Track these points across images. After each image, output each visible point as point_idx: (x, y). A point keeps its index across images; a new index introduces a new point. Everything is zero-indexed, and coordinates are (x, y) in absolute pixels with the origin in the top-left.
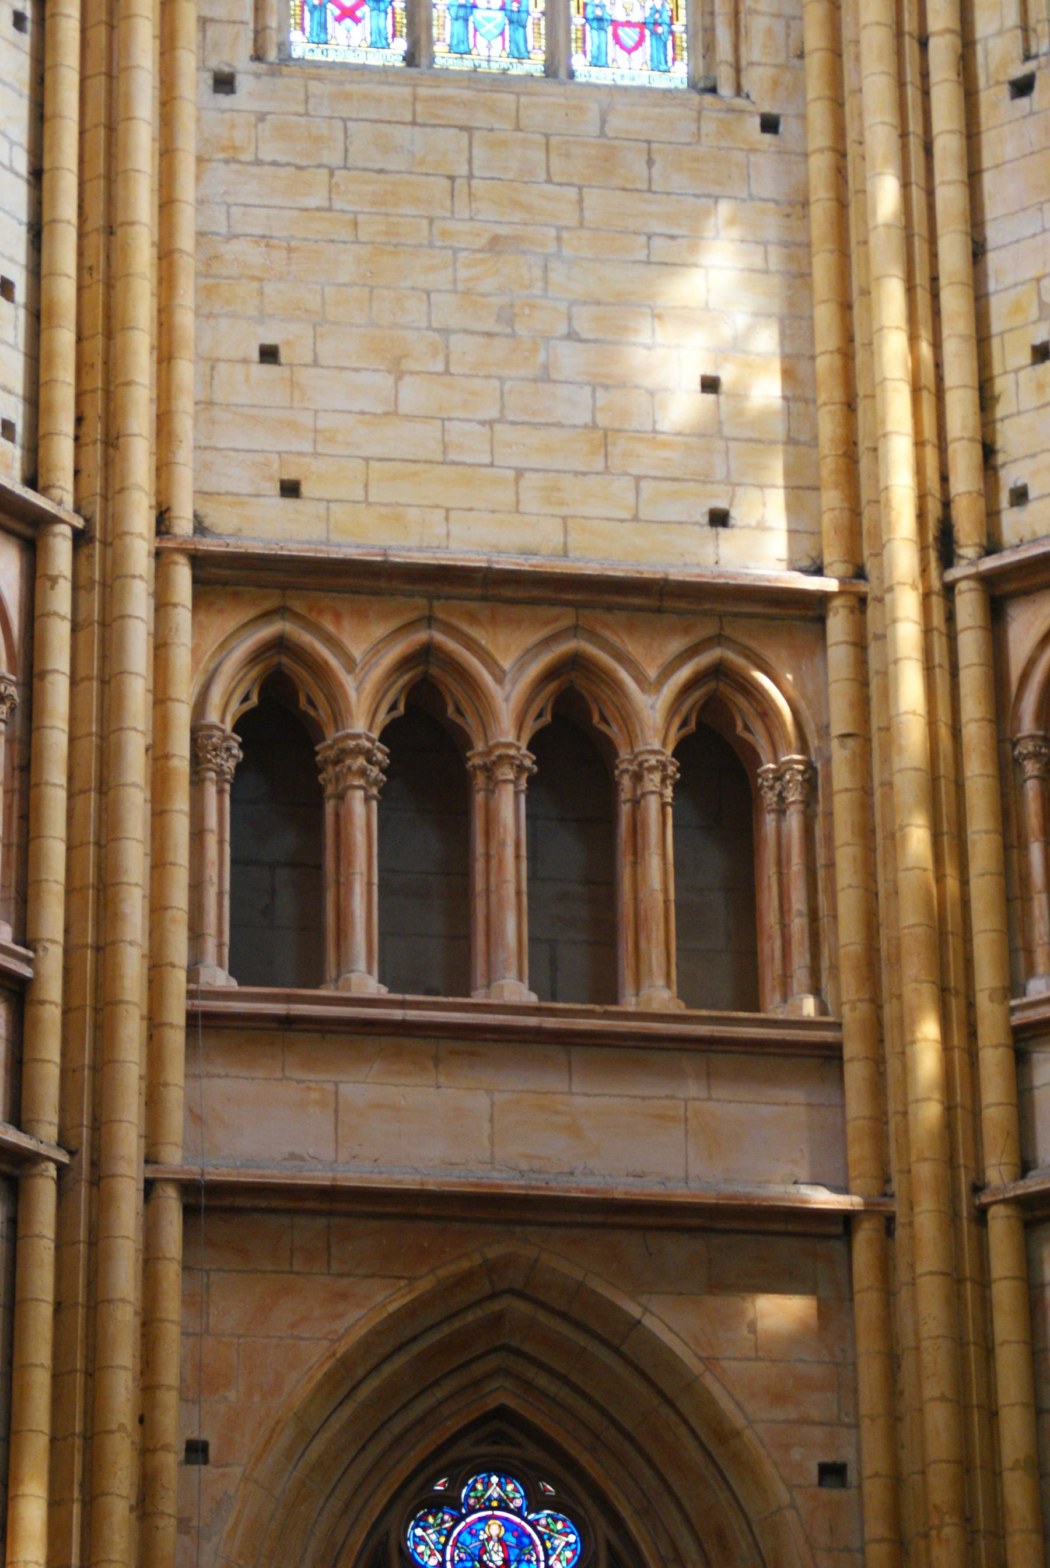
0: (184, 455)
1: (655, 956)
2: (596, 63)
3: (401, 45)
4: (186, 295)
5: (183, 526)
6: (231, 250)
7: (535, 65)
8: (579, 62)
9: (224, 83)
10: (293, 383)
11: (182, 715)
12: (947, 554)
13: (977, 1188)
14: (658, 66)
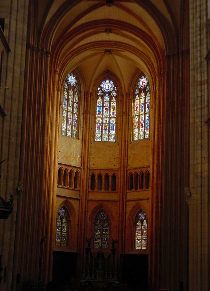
2: (111, 140)
3: (101, 140)
7: (107, 140)
8: (110, 140)
9: (91, 143)
10: (94, 159)
11: (88, 177)
13: (124, 200)
14: (114, 140)
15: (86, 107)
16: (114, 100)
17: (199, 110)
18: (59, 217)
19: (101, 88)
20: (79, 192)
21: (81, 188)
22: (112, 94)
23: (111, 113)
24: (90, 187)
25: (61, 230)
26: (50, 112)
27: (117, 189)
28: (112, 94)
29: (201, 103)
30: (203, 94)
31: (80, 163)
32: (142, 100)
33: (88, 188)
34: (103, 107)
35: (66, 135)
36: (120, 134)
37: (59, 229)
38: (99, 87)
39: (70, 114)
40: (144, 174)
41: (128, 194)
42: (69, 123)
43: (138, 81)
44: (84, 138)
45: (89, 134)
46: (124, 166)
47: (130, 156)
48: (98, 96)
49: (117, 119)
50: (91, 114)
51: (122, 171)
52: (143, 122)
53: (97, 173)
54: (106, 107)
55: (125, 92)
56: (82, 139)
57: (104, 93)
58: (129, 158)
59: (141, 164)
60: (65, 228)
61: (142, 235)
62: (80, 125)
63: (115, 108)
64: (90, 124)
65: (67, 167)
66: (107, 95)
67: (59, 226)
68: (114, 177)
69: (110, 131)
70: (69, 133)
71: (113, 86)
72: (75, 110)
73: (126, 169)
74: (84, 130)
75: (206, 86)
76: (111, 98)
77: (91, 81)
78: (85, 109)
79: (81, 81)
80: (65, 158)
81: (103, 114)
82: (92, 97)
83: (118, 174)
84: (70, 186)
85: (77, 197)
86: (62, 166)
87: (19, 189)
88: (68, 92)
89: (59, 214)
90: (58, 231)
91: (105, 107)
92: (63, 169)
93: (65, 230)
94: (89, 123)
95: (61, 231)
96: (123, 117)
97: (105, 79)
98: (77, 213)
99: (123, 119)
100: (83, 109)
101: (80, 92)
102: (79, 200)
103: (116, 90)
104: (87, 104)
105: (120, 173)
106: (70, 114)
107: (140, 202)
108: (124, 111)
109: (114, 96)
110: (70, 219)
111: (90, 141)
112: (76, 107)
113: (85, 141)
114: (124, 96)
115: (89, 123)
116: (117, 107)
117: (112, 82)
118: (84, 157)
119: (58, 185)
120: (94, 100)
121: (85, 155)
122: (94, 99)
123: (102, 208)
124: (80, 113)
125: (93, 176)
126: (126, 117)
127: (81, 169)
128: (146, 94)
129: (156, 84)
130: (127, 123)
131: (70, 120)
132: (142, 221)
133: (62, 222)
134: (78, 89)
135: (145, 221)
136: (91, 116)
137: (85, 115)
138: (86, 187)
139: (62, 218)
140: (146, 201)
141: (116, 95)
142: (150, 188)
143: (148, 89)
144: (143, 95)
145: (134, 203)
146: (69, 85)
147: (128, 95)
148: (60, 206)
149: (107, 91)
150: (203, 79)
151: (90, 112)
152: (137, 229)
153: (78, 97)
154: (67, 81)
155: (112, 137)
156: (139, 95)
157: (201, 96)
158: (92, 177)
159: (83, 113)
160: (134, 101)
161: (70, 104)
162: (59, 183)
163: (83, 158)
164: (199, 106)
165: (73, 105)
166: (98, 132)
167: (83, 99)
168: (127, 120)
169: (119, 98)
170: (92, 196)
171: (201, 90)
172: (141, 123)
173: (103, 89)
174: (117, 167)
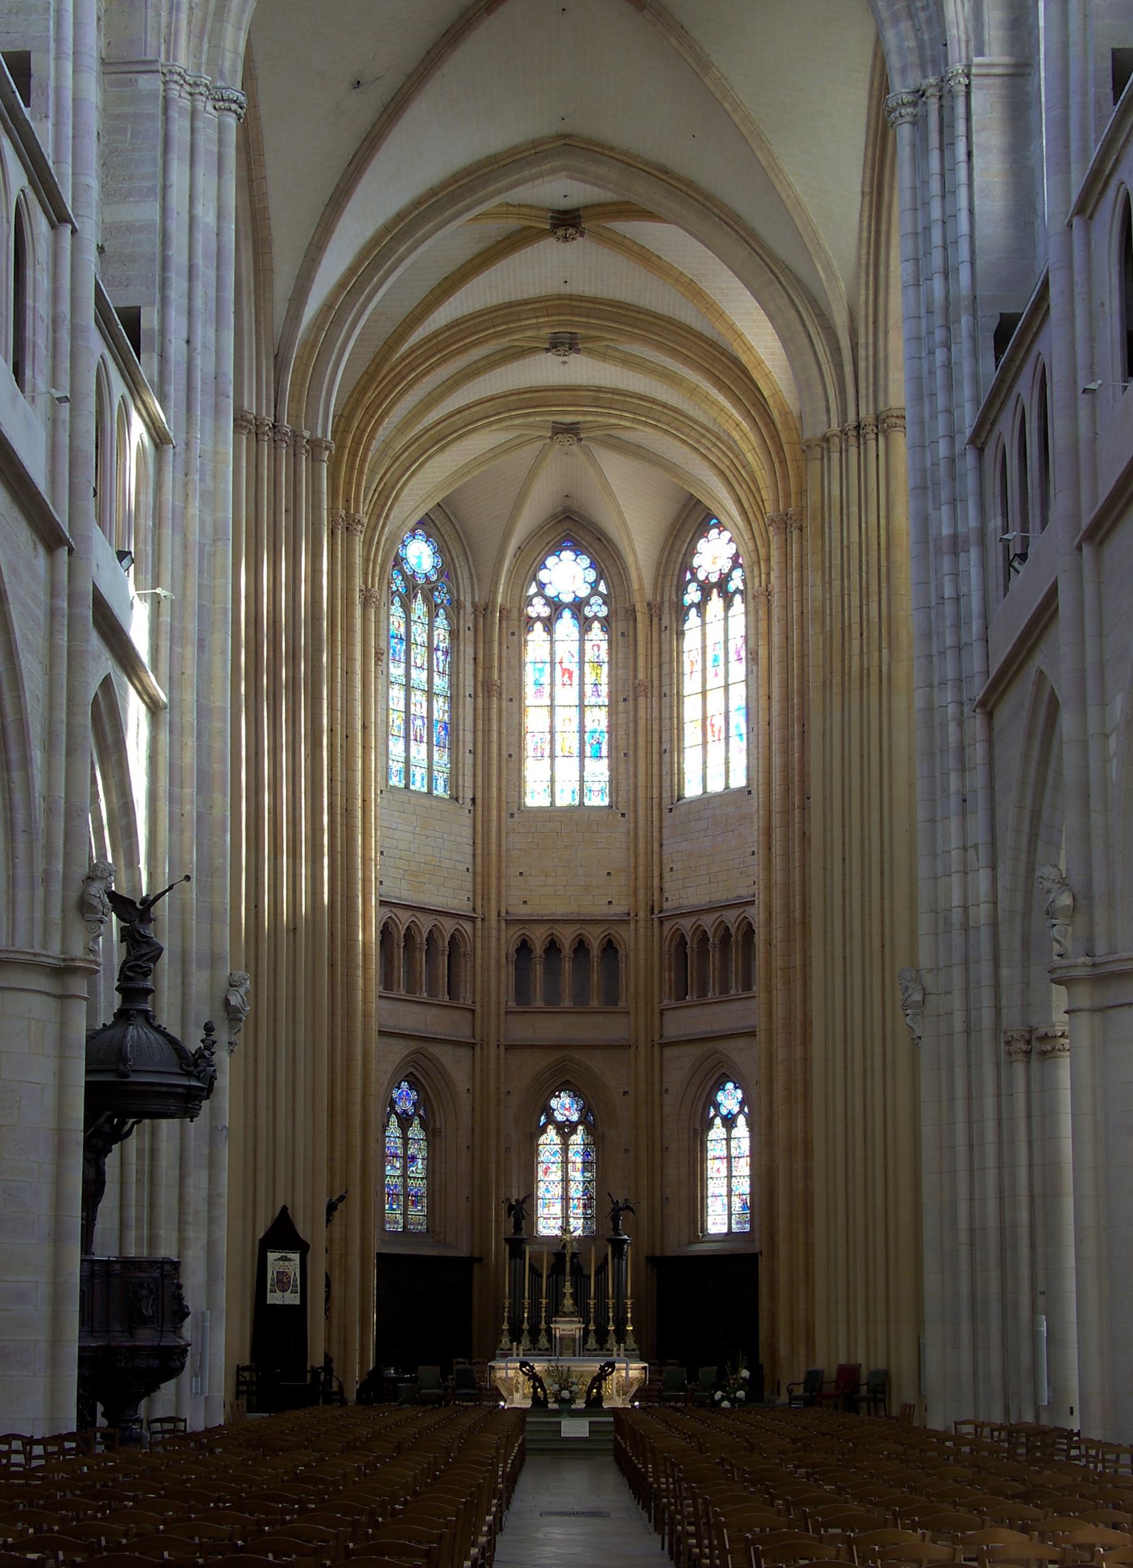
0: (503, 899)
1: (595, 995)
4: (504, 865)
5: (503, 913)
6: (514, 852)
9: (512, 815)
11: (503, 953)
12: (652, 913)
15: (483, 663)
16: (596, 632)
17: (950, 655)
18: (393, 1118)
19: (542, 586)
20: (468, 1015)
21: (478, 998)
22: (588, 612)
23: (588, 689)
24: (512, 988)
25: (405, 1168)
26: (337, 692)
27: (624, 998)
28: (588, 612)
29: (957, 626)
30: (963, 589)
32: (715, 632)
33: (503, 999)
34: (552, 664)
35: (407, 786)
36: (628, 770)
37: (393, 1167)
38: (534, 584)
39: (418, 698)
40: (733, 931)
41: (668, 1016)
42: (416, 735)
43: (692, 551)
44: (479, 796)
45: (499, 778)
46: (650, 902)
47: (673, 861)
48: (530, 622)
49: (612, 709)
50: (504, 696)
51: (641, 924)
52: (719, 722)
53: (538, 937)
54: (564, 666)
55: (642, 596)
56: (474, 800)
57: (556, 606)
58: (669, 870)
59: (720, 894)
60: (420, 1161)
61: (730, 1177)
63: (605, 667)
64: (504, 736)
66: (567, 614)
67: (396, 1156)
68: (610, 947)
69: (587, 761)
70: (418, 778)
71: (592, 575)
72: (441, 683)
73: (657, 915)
74: (479, 762)
75: (974, 554)
76: (585, 625)
77: (499, 562)
78: (480, 678)
79: (459, 562)
80: (406, 877)
81: (552, 696)
82: (504, 623)
83: (625, 936)
84: (432, 991)
85: (464, 1034)
86: (394, 910)
87: (235, 1000)
88: (407, 609)
89: (392, 1103)
90: (392, 1173)
91: (561, 663)
93: (418, 1168)
95: (405, 1176)
96: (636, 700)
97: (556, 549)
98: (465, 1100)
99: (636, 710)
100: (472, 678)
101: (455, 608)
102: (472, 1046)
103: (605, 592)
104: (488, 655)
105: (632, 932)
106: (418, 698)
107: (721, 1046)
108: (641, 675)
109: (596, 617)
110: (438, 1125)
111: (504, 804)
112: (441, 670)
113: (487, 809)
114: (639, 616)
115: (500, 733)
116: (610, 662)
117: (585, 561)
118: (486, 876)
119: (381, 989)
120: (515, 638)
121: (486, 864)
122: (513, 634)
123: (567, 1078)
124: (461, 692)
125: (524, 947)
126: (649, 700)
127: (473, 920)
128: (728, 605)
129: (768, 560)
130: (656, 727)
131: (419, 722)
132: (729, 1122)
133: (405, 1139)
134: (449, 592)
135: (741, 1120)
136: (504, 702)
137: (480, 700)
138: (498, 991)
139: (405, 1122)
140: (742, 1043)
141: (603, 611)
142: (758, 987)
143: (736, 583)
144: (716, 604)
145: (695, 1050)
146: (410, 580)
147: (654, 610)
148: (396, 1073)
149: (567, 598)
150: (960, 529)
151: (500, 687)
152: (710, 1155)
153: (450, 625)
154: (399, 561)
155: (596, 787)
156: (701, 607)
157: (957, 599)
158: (518, 951)
159: (472, 693)
160: (681, 634)
161: (419, 655)
162: (387, 981)
163: (479, 879)
164: (949, 641)
165: (428, 661)
166: (535, 773)
167: (470, 635)
168: (656, 714)
169: (620, 626)
170: (523, 1030)
171: (955, 574)
172: (713, 726)
173: (550, 592)
174: (619, 909)
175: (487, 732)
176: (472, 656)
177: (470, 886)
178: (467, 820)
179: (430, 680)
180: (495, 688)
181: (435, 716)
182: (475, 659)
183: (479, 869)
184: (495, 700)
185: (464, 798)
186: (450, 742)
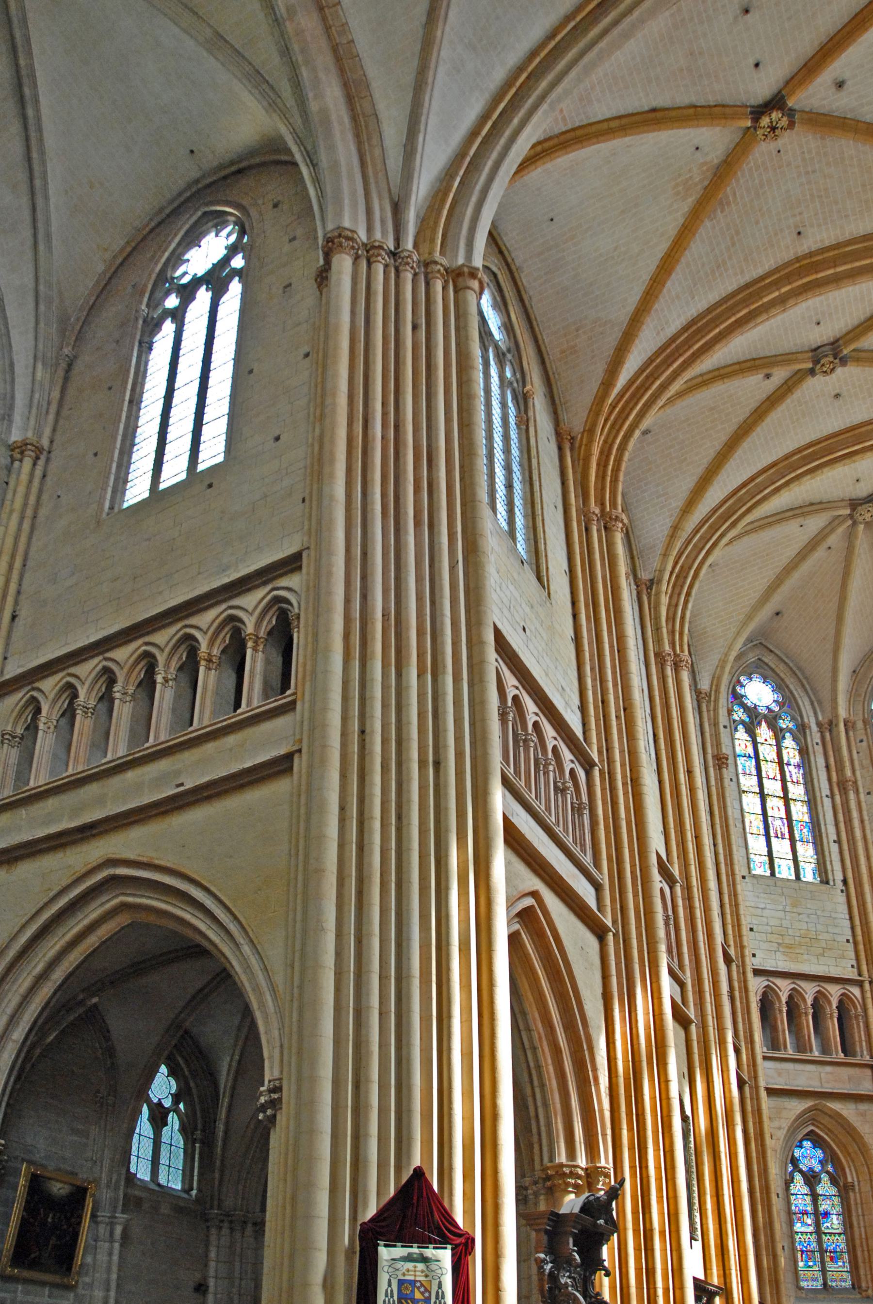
31: (853, 966)
50: (861, 790)
62: (824, 835)
65: (799, 982)
72: (797, 791)
74: (845, 847)
86: (771, 979)
92: (781, 994)
94: (862, 821)
101: (800, 732)
115: (862, 821)
124: (818, 794)
134: (793, 719)
136: (862, 796)
137: (838, 798)
146: (752, 712)
153: (798, 744)
154: (737, 698)
159: (829, 793)
161: (770, 769)
167: (819, 749)
175: (849, 821)
176: (824, 764)
177: (852, 955)
178: (842, 898)
179: (785, 789)
180: (850, 783)
181: (795, 817)
182: (827, 767)
183: (860, 938)
184: (852, 796)
185: (834, 880)
186: (814, 837)
